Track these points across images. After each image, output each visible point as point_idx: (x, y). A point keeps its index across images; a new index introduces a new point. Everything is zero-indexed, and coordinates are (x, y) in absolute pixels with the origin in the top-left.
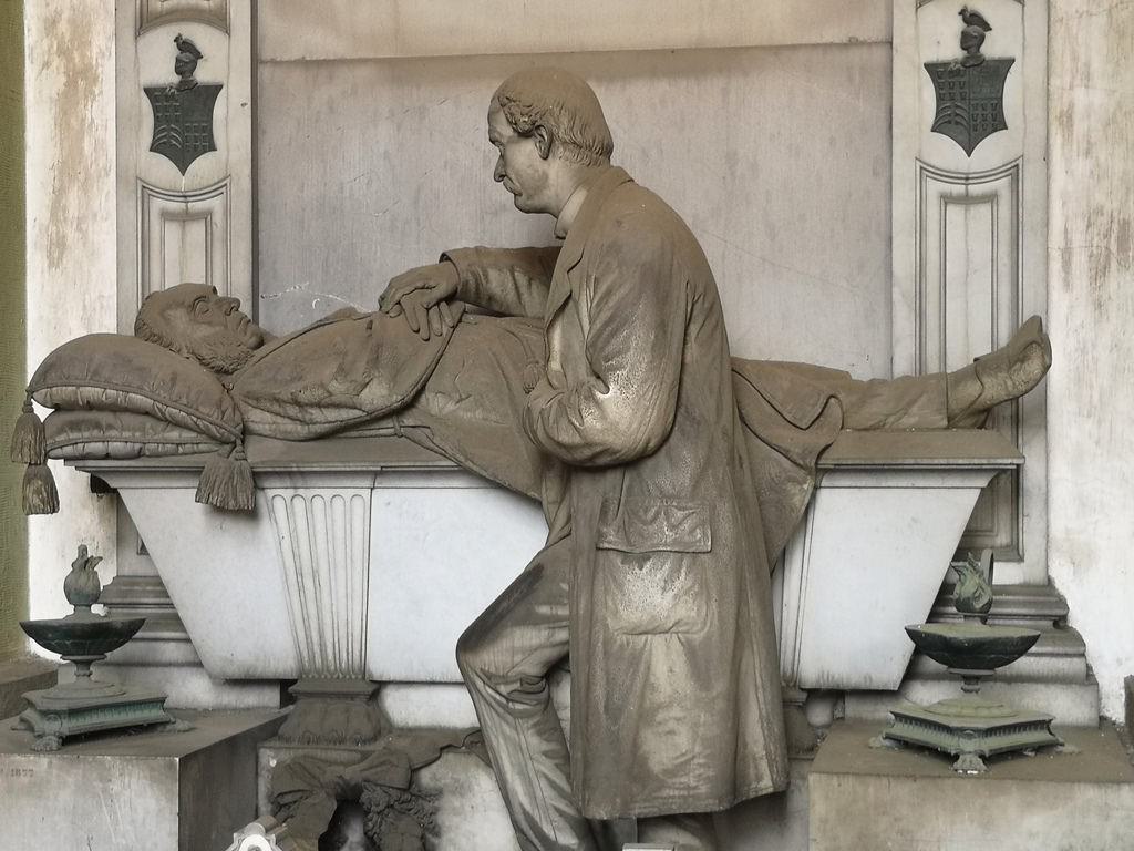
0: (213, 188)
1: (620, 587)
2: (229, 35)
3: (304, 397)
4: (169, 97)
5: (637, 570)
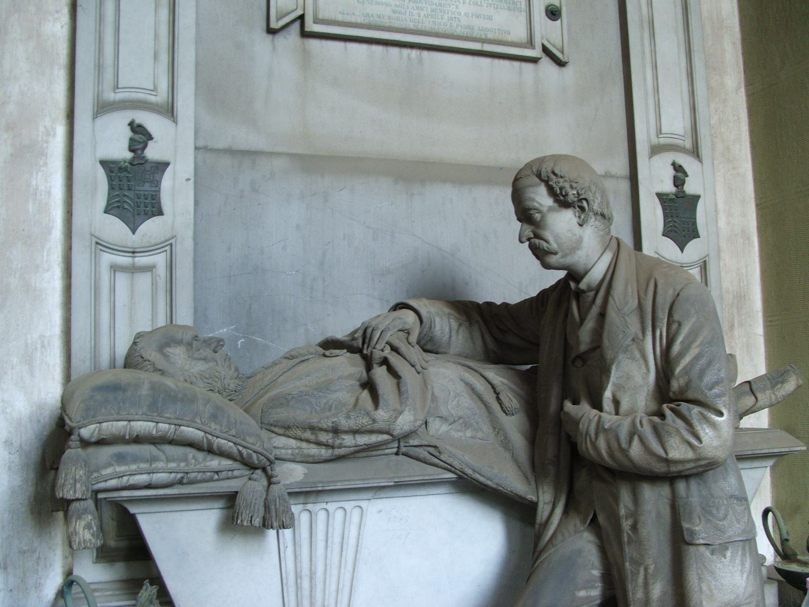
0: (160, 246)
1: (712, 573)
2: (175, 121)
3: (344, 424)
4: (121, 169)
5: (723, 559)
